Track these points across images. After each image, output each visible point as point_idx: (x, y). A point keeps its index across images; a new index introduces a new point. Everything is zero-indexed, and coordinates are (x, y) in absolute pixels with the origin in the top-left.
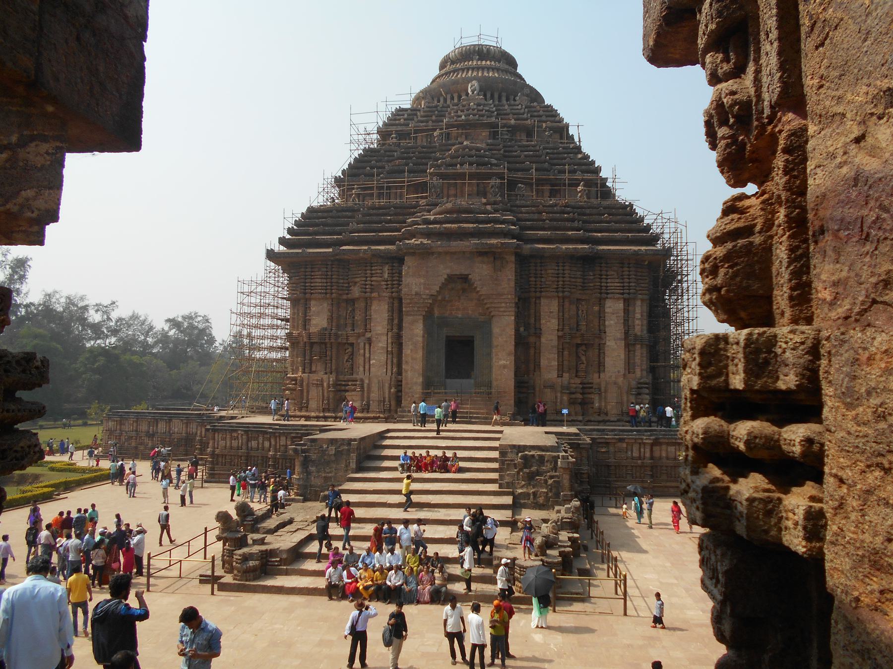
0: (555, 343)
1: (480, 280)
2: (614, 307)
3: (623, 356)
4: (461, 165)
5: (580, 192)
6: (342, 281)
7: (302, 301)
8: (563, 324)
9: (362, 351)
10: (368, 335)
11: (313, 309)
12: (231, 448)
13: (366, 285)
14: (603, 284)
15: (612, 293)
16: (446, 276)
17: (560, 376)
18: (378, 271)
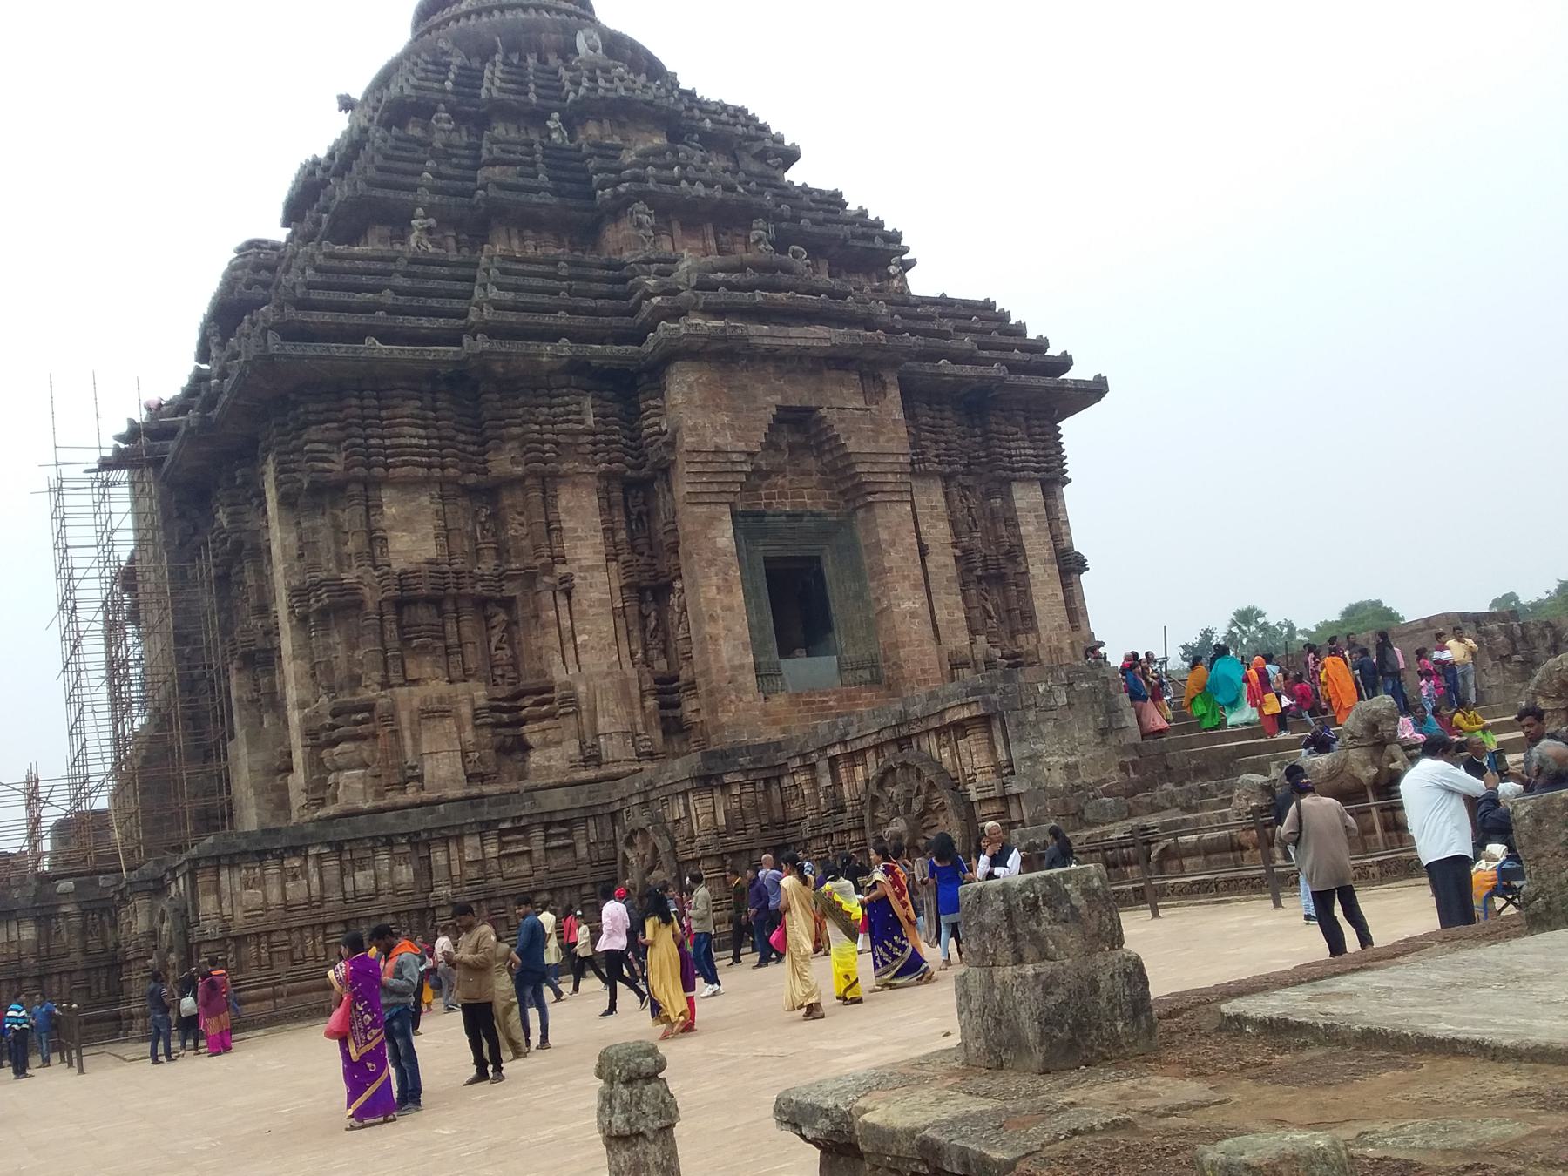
0: (953, 572)
1: (842, 420)
2: (1026, 497)
3: (1061, 596)
4: (692, 183)
5: (894, 277)
6: (462, 437)
7: (354, 489)
8: (956, 534)
9: (552, 613)
10: (561, 570)
11: (391, 510)
12: (286, 906)
13: (543, 442)
14: (1006, 452)
15: (1021, 470)
16: (774, 411)
17: (973, 642)
18: (574, 408)
